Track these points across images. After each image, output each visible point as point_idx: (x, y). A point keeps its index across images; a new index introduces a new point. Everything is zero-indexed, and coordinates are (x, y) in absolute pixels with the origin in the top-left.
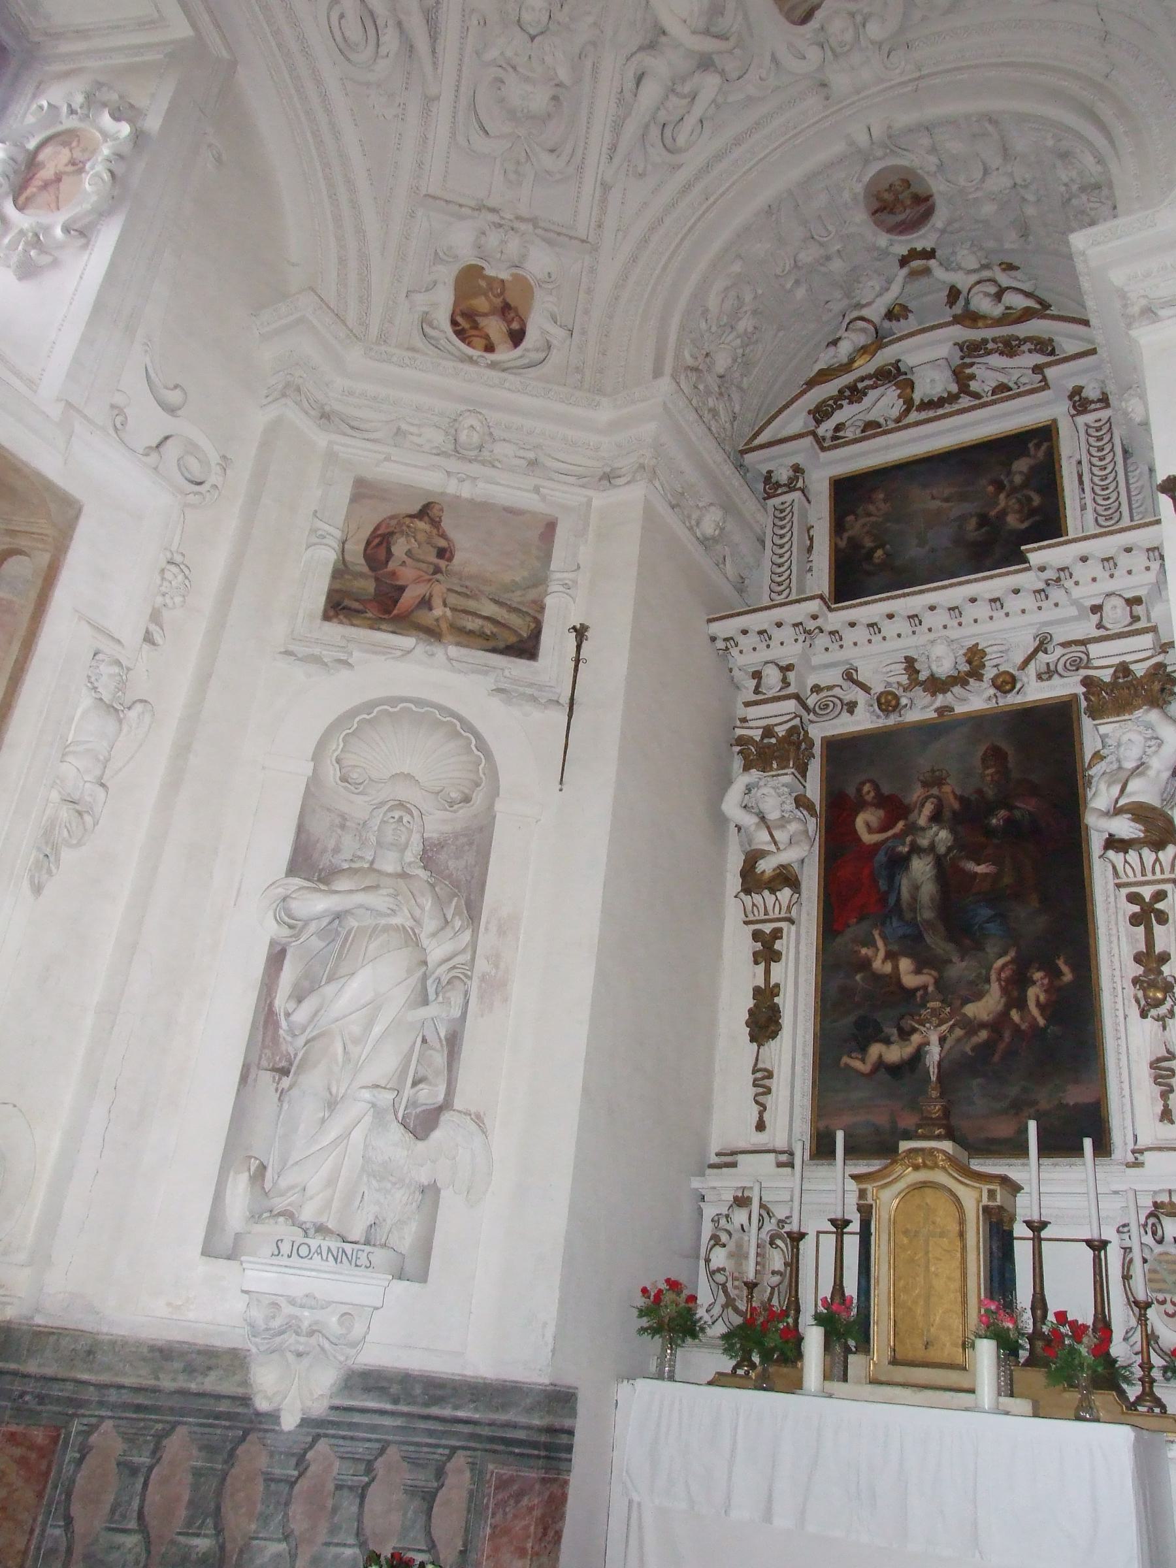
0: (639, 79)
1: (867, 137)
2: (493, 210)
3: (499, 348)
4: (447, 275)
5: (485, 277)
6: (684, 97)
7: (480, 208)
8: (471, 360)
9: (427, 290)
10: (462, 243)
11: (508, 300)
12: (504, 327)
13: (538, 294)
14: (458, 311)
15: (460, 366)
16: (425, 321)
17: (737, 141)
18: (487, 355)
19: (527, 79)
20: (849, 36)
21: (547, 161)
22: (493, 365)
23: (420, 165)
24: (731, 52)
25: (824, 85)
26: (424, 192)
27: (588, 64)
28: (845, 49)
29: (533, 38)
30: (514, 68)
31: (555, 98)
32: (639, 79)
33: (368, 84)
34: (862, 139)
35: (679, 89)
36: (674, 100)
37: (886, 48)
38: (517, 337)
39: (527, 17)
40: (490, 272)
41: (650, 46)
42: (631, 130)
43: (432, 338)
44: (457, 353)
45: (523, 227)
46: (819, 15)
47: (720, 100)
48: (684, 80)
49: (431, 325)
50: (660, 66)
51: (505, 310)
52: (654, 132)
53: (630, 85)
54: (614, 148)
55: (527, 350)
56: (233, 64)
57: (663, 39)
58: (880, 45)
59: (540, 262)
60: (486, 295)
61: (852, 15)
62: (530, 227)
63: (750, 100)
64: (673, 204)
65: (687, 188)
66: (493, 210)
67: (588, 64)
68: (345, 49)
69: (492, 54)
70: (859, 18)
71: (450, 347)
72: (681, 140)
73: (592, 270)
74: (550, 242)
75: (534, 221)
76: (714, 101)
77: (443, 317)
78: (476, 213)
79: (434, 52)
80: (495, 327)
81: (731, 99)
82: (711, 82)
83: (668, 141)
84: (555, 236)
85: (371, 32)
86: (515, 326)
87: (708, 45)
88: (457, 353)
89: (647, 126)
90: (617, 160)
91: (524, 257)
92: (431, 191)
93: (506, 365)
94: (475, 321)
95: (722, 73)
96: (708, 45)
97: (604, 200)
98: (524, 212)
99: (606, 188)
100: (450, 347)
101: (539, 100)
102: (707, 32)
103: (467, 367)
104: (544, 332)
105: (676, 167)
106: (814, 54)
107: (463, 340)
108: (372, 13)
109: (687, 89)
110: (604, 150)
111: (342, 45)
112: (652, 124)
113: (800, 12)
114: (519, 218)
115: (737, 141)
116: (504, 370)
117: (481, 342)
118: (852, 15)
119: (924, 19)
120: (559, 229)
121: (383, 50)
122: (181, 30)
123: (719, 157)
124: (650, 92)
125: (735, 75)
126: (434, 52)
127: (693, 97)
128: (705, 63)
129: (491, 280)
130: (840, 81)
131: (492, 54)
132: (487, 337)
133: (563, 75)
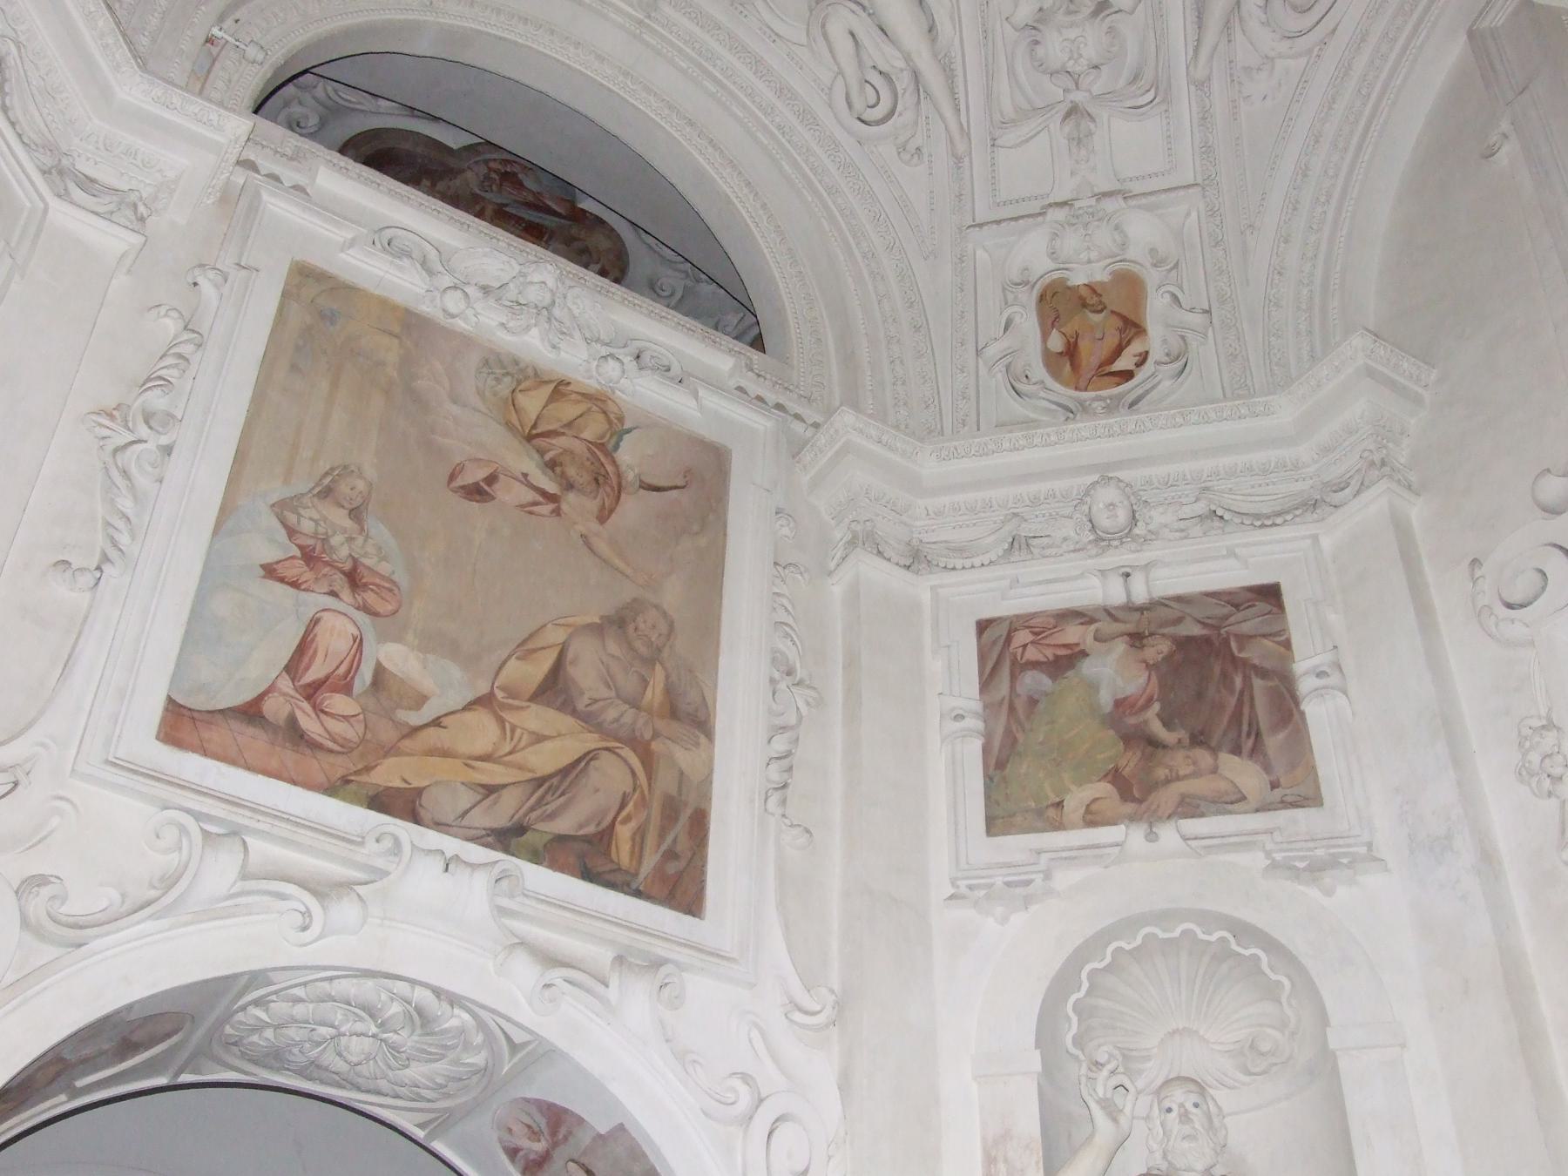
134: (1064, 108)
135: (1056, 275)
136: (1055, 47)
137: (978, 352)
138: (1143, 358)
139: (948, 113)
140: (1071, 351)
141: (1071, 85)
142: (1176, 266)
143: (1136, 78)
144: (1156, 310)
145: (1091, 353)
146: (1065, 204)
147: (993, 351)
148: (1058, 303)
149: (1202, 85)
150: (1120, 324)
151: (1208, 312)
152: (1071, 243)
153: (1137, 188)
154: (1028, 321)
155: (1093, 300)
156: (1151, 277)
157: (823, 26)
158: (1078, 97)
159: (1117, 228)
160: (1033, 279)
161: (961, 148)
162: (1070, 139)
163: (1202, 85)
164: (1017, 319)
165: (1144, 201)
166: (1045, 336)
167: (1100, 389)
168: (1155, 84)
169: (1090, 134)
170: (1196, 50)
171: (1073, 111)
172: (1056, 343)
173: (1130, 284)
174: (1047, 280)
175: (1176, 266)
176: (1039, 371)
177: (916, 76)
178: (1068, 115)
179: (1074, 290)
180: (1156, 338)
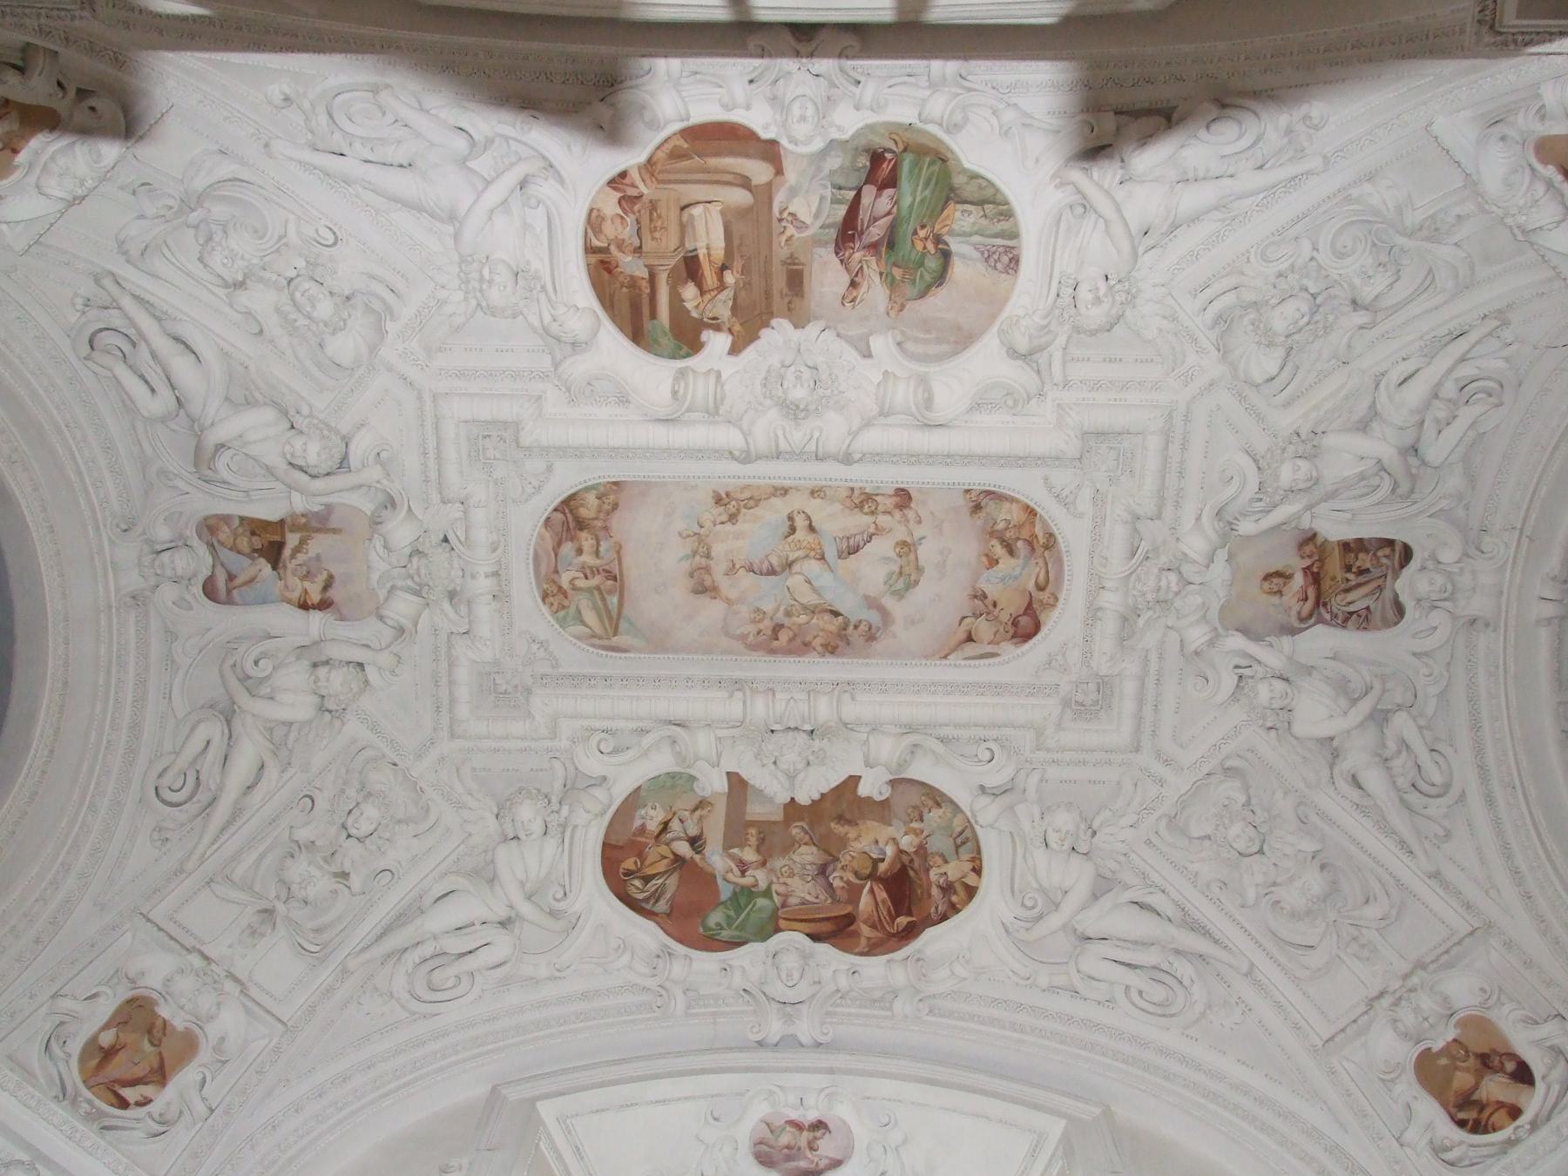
0: (1355, 782)
1: (1550, 604)
2: (1381, 995)
3: (1521, 1101)
4: (1408, 1087)
5: (1441, 1053)
6: (1399, 752)
7: (1371, 1002)
8: (1511, 1143)
9: (1409, 1121)
10: (1390, 1047)
11: (1480, 1051)
12: (1501, 1079)
13: (1493, 1015)
14: (1453, 1110)
15: (1506, 1160)
16: (1438, 1150)
17: (1476, 727)
18: (1519, 1122)
19: (1291, 879)
20: (1440, 580)
21: (1372, 912)
22: (1534, 1126)
23: (1297, 1027)
24: (1384, 691)
25: (1473, 622)
26: (1320, 1044)
27: (1314, 818)
28: (1449, 587)
29: (1261, 852)
30: (1275, 884)
31: (1323, 867)
32: (1355, 782)
33: (1203, 1014)
34: (1549, 610)
35: (1388, 753)
36: (1397, 763)
37: (1472, 551)
38: (1523, 1075)
39: (1241, 845)
40: (1438, 1045)
41: (1336, 755)
42: (1398, 820)
43: (1461, 1159)
44: (1492, 1150)
45: (1415, 980)
46: (1403, 598)
47: (1422, 722)
48: (1384, 746)
49: (1448, 1149)
50: (1357, 757)
51: (1487, 1062)
52: (1413, 798)
53: (1355, 794)
54: (1402, 844)
55: (1544, 1077)
56: (1107, 1113)
57: (1335, 743)
58: (1466, 555)
59: (1463, 990)
60: (1457, 1068)
61: (1423, 568)
62: (1420, 973)
63: (1443, 695)
64: (1497, 823)
65: (1490, 801)
66: (1381, 995)
67: (1314, 818)
68: (1163, 1011)
69: (1251, 894)
70: (1430, 565)
71: (1485, 1151)
72: (1438, 778)
73: (1509, 945)
74: (1450, 966)
75: (1420, 965)
76: (1420, 728)
77: (1447, 1130)
78: (1372, 1013)
79: (1216, 942)
80: (1495, 1088)
81: (1430, 710)
82: (1402, 723)
83: (1434, 791)
84: (1448, 957)
85: (1167, 979)
86: (1510, 1066)
87: (1365, 706)
88: (1492, 1150)
89: (1402, 800)
90: (1416, 847)
91: (1446, 999)
92: (1325, 1038)
93: (1545, 1112)
94: (1475, 1103)
95: (1400, 707)
96: (1365, 706)
97: (1446, 885)
98: (1405, 967)
99: (1435, 875)
100: (1485, 1151)
101: (1314, 882)
102: (1354, 702)
103: (1514, 1154)
104: (1537, 1043)
105: (1462, 796)
106: (1437, 618)
107: (1486, 1131)
108: (1154, 967)
109: (1392, 746)
110: (1399, 854)
111: (1159, 1011)
112: (1406, 796)
113: (1390, 613)
114: (1406, 977)
115: (1476, 727)
116: (1549, 1118)
117: (1499, 1117)
118: (1423, 568)
119: (1467, 508)
120: (1443, 949)
121: (1186, 982)
122: (1057, 1128)
123: (1479, 751)
124: (1374, 779)
125: (1409, 695)
126: (1216, 942)
127: (1404, 744)
128: (1380, 718)
129: (1445, 1051)
130: (1478, 605)
131: (1251, 894)
132: (1501, 1105)
133: (1309, 846)
134: (269, 906)
135: (155, 995)
136: (299, 868)
137: (54, 996)
138: (145, 1102)
139: (206, 839)
140: (108, 1054)
141: (284, 895)
142: (224, 1062)
143: (317, 931)
144: (185, 1078)
145: (119, 1067)
146: (206, 958)
147: (65, 1004)
148: (138, 1014)
149: (345, 972)
150: (156, 1066)
151: (212, 1111)
152: (185, 984)
153: (254, 992)
154: (106, 1008)
155: (157, 1033)
156: (205, 1055)
157: (199, 722)
158: (281, 908)
159: (219, 1004)
160: (140, 983)
161: (190, 866)
162: (250, 926)
163: (345, 972)
164: (102, 1000)
165: (249, 1004)
166: (106, 1027)
167: (99, 1097)
168: (325, 946)
169: (263, 935)
170: (364, 950)
171: (268, 912)
172: (107, 1039)
173: (189, 1045)
174: (145, 992)
175: (224, 1062)
176: (76, 1047)
177: (213, 801)
178: (265, 911)
179: (155, 1015)
180: (165, 1098)
